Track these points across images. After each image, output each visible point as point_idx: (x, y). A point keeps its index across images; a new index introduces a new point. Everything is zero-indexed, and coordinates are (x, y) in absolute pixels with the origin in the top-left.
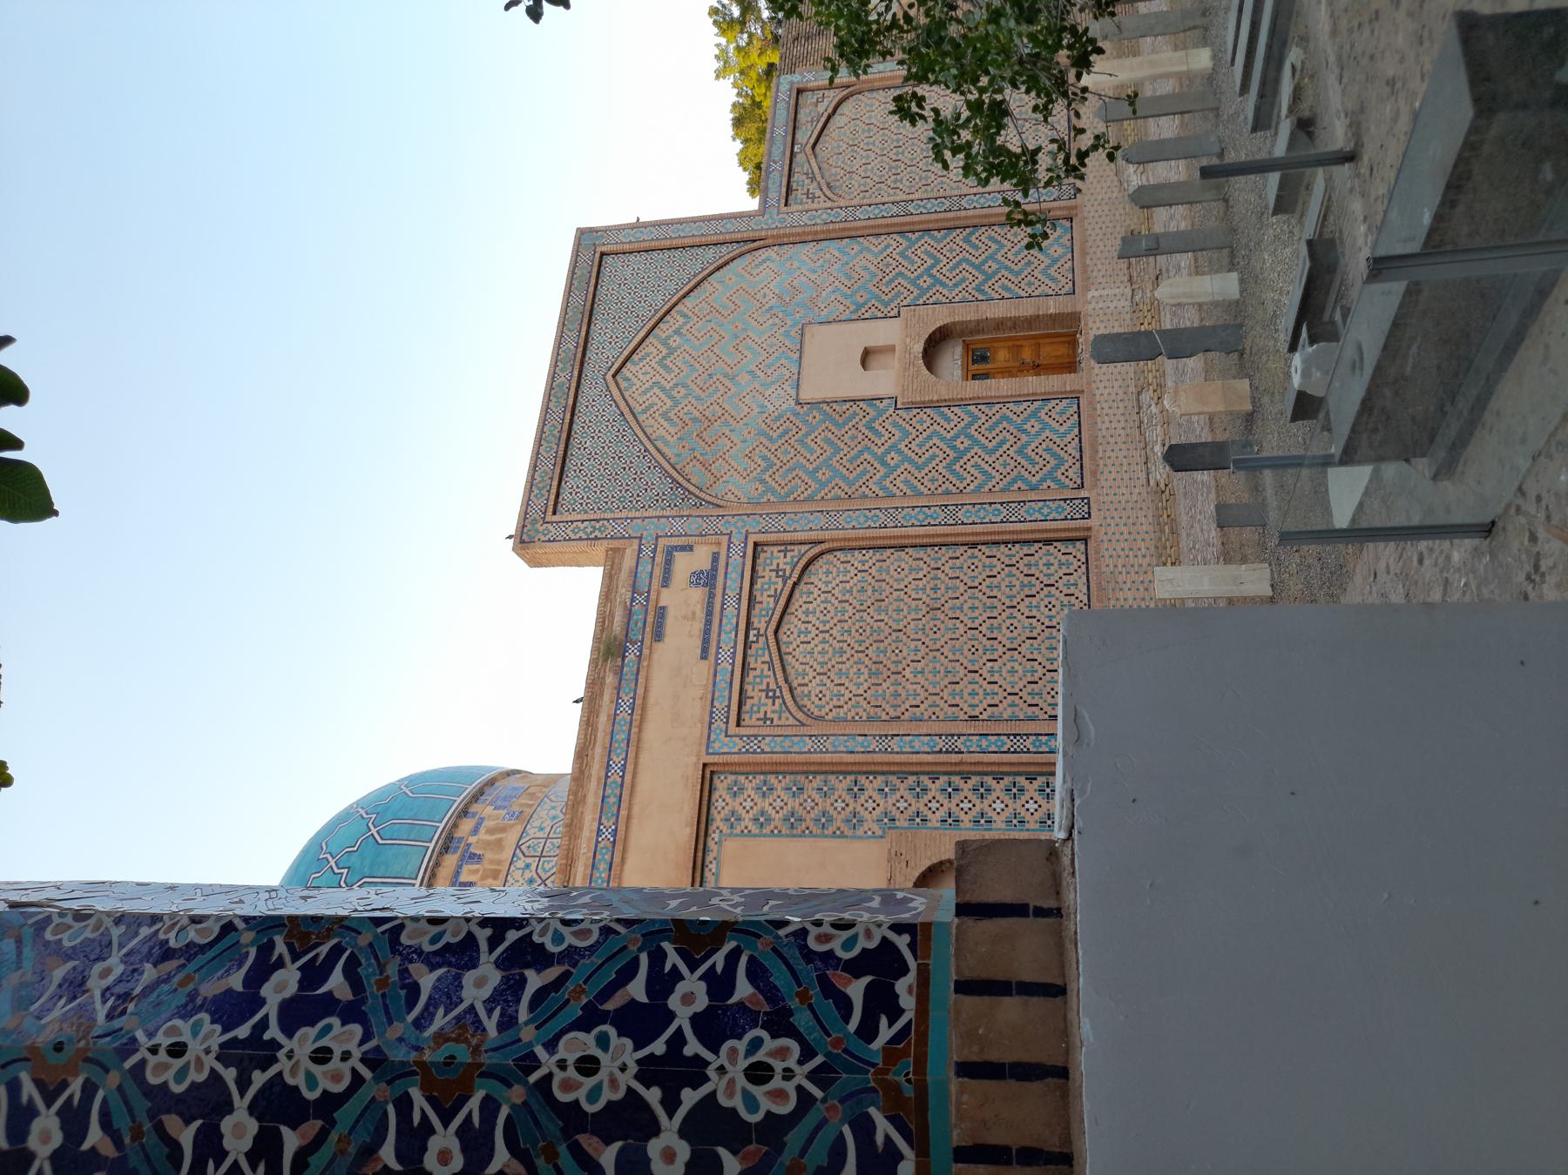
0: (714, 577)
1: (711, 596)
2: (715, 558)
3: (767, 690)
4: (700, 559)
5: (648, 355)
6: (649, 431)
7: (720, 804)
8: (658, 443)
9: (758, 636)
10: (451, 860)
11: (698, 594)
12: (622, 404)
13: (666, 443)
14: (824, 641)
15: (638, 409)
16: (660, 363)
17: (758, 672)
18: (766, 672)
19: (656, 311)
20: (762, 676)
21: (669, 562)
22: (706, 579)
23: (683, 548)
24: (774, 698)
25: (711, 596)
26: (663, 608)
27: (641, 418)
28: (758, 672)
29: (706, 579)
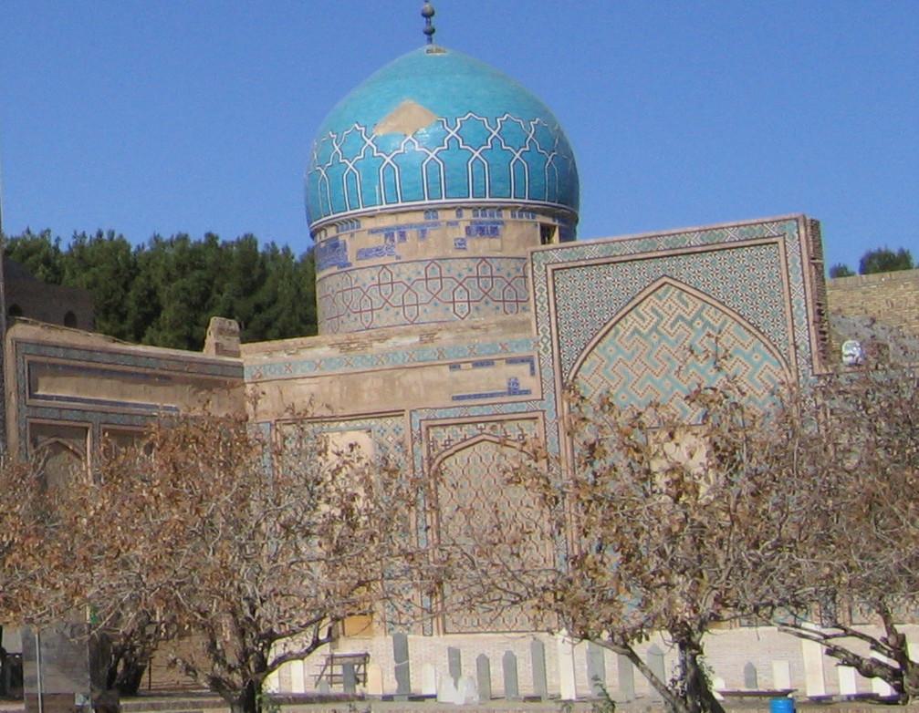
0: (515, 394)
1: (502, 394)
2: (527, 392)
3: (450, 440)
4: (527, 382)
5: (687, 306)
6: (622, 322)
7: (389, 422)
8: (613, 331)
9: (481, 429)
10: (420, 218)
11: (504, 384)
12: (642, 296)
13: (615, 336)
14: (482, 471)
15: (640, 309)
16: (680, 317)
17: (459, 432)
18: (460, 437)
19: (723, 304)
20: (457, 435)
21: (523, 360)
22: (514, 389)
23: (532, 368)
24: (445, 445)
25: (502, 394)
26: (493, 364)
27: (632, 313)
28: (459, 432)
29: (514, 389)
